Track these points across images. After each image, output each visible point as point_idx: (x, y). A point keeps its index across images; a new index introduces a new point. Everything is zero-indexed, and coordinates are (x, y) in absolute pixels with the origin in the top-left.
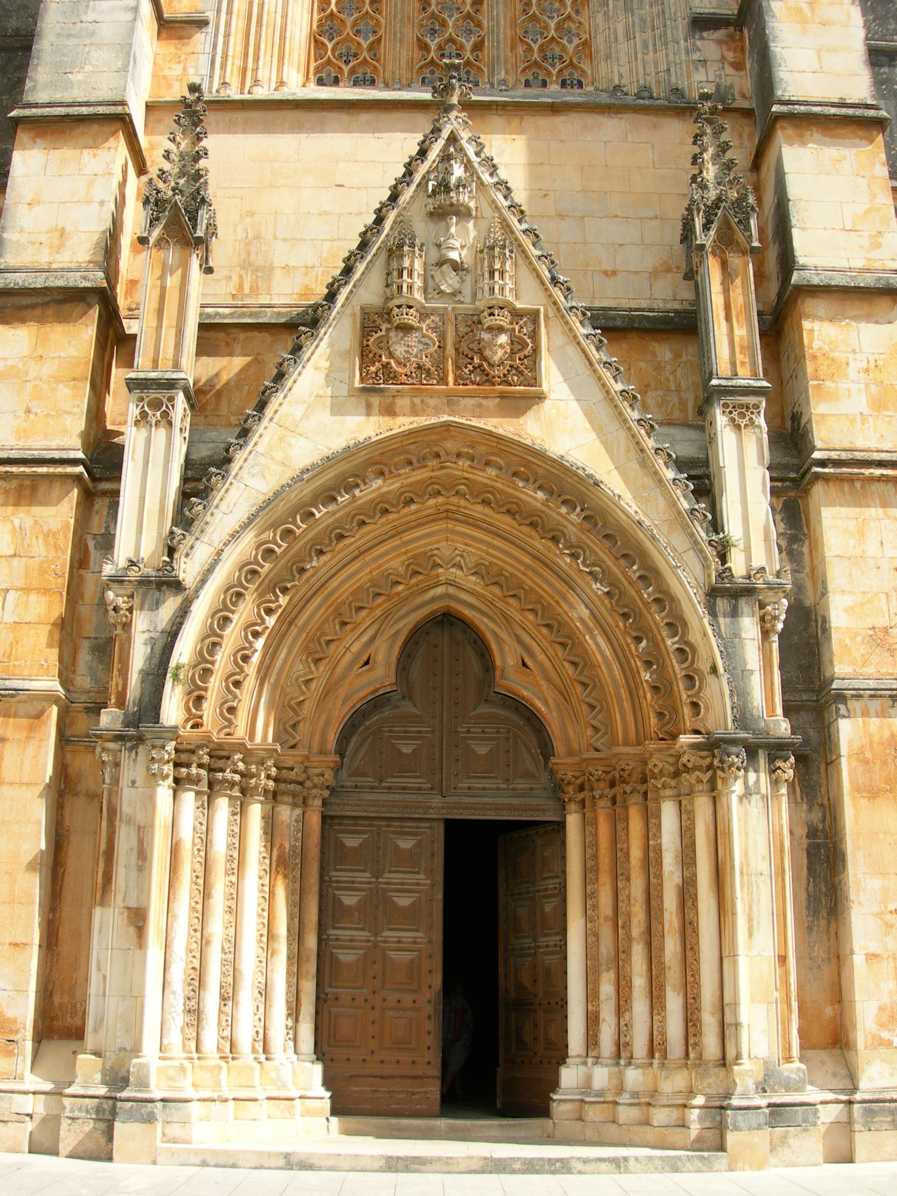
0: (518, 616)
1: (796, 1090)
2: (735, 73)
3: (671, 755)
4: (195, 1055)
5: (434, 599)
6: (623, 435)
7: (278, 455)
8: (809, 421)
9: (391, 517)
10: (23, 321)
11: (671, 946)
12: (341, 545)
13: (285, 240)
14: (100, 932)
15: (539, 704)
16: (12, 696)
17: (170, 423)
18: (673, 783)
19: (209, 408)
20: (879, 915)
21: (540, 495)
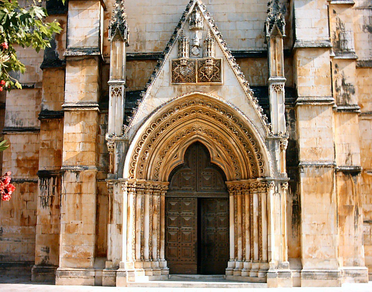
0: (216, 143)
3: (256, 182)
7: (151, 104)
9: (181, 119)
10: (77, 65)
11: (255, 232)
13: (149, 32)
15: (222, 167)
17: (121, 95)
18: (256, 190)
19: (130, 85)
20: (309, 224)
21: (221, 113)
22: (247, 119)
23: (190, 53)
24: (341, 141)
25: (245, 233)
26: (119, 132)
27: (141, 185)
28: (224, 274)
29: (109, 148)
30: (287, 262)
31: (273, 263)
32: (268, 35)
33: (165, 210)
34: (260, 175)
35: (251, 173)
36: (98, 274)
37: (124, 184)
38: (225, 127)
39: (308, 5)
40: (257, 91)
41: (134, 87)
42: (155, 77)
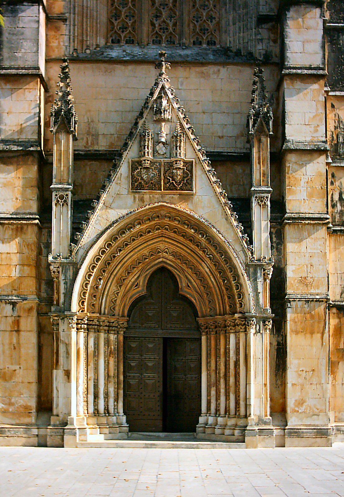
8: (286, 201)
9: (143, 237)
13: (102, 123)
14: (56, 380)
18: (233, 328)
22: (224, 239)
23: (155, 151)
24: (336, 269)
25: (219, 381)
26: (66, 253)
27: (93, 321)
28: (194, 431)
29: (52, 273)
30: (269, 417)
31: (253, 417)
32: (252, 131)
33: (124, 353)
35: (228, 308)
36: (42, 432)
37: (73, 319)
38: (197, 249)
39: (301, 94)
40: (237, 204)
41: (85, 195)
42: (110, 182)
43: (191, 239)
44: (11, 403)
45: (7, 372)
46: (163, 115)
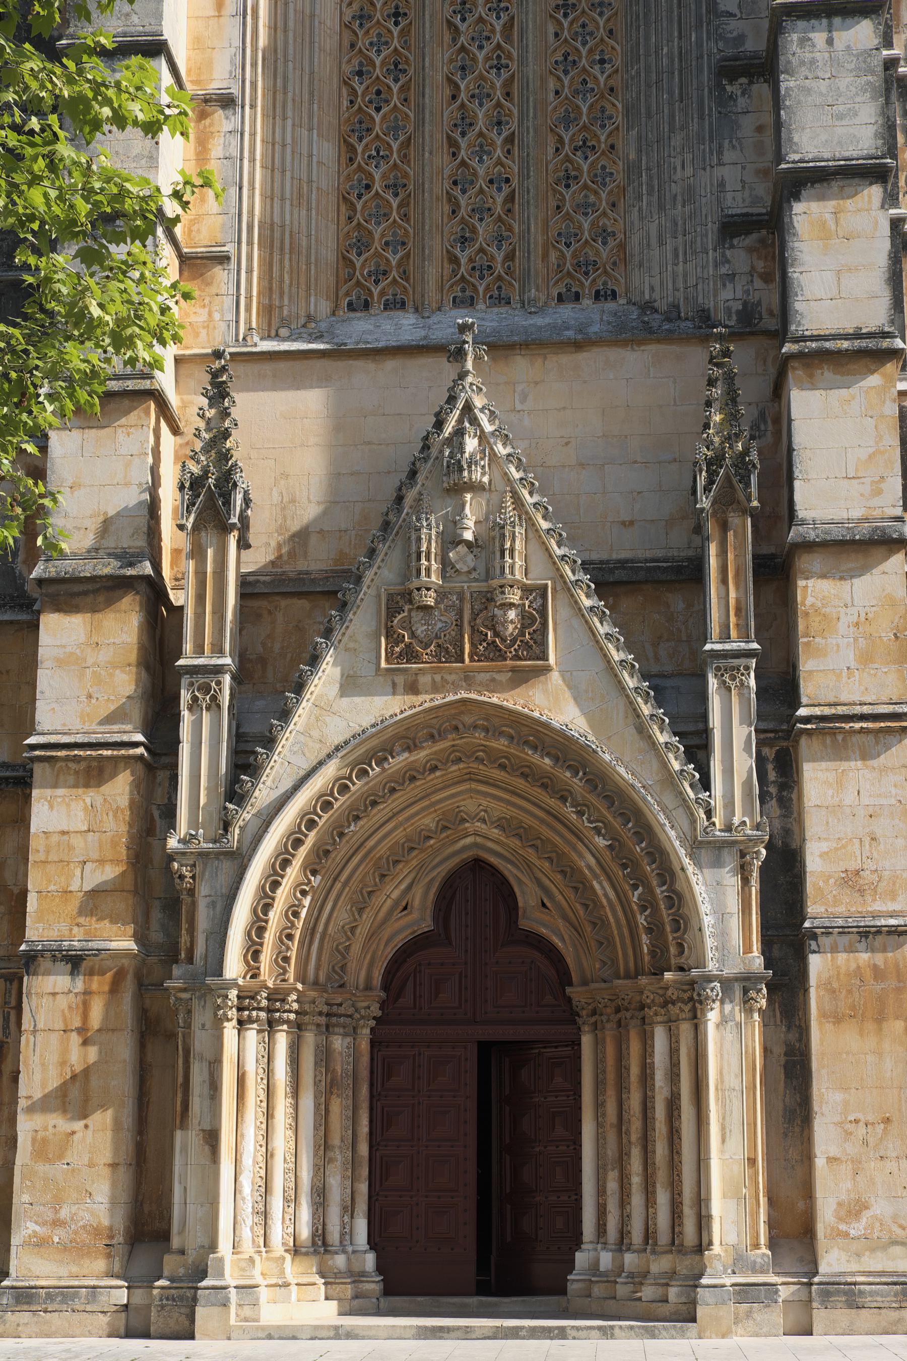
1: (762, 1272)
2: (764, 286)
4: (264, 1250)
5: (465, 848)
6: (621, 703)
7: (315, 734)
9: (418, 783)
12: (375, 811)
16: (95, 955)
17: (219, 706)
18: (663, 1011)
21: (547, 761)
23: (446, 564)
29: (177, 881)
30: (765, 1250)
32: (705, 503)
34: (673, 961)
37: (227, 996)
43: (547, 783)
44: (58, 1220)
45: (51, 1137)
46: (466, 474)
